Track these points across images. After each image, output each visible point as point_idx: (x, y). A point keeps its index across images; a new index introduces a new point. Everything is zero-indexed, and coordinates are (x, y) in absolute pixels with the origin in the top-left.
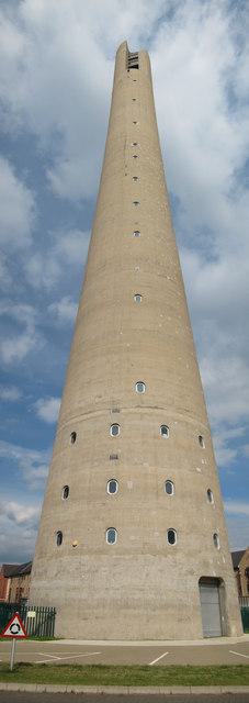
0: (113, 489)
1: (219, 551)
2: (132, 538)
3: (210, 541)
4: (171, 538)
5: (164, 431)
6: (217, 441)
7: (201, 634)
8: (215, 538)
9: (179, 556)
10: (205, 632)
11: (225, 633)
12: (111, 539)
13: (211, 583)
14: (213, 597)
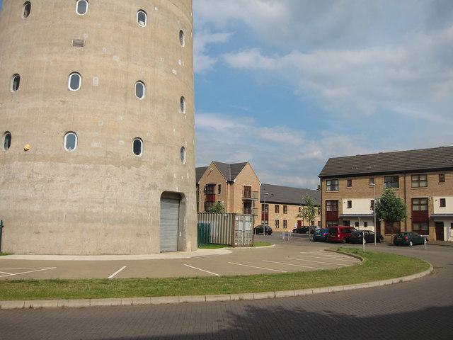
0: (75, 84)
1: (185, 165)
2: (95, 145)
3: (177, 155)
4: (137, 147)
5: (142, 18)
6: (198, 43)
7: (158, 249)
8: (182, 101)
9: (144, 169)
10: (161, 247)
11: (180, 248)
12: (71, 144)
13: (171, 198)
14: (173, 211)
